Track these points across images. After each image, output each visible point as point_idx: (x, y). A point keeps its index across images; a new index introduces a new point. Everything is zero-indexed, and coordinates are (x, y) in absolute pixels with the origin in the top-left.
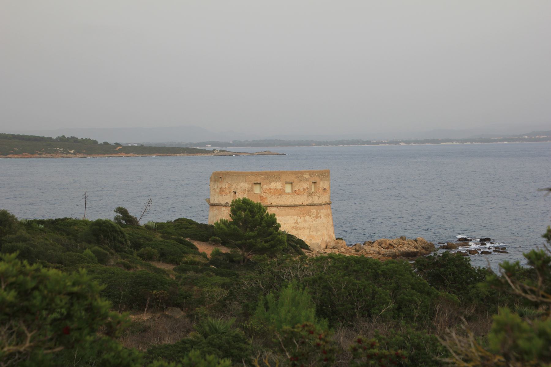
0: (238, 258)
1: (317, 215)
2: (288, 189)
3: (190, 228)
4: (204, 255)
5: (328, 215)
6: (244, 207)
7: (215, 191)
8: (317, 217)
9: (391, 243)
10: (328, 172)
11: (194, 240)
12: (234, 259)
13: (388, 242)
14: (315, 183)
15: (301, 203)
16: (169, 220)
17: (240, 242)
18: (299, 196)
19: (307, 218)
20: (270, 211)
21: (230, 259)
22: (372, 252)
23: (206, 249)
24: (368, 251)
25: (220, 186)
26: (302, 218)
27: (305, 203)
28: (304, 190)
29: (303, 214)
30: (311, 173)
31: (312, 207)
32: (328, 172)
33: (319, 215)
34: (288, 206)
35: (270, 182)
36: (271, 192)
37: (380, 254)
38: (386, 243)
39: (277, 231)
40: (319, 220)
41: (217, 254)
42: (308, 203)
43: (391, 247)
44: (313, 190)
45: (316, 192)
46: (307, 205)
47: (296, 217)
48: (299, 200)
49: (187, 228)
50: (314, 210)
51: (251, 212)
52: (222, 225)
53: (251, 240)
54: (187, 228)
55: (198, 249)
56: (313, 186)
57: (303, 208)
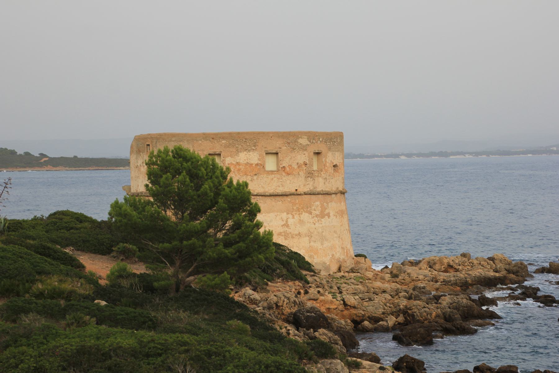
0: (163, 283)
1: (322, 212)
2: (271, 164)
3: (77, 229)
4: (92, 280)
5: (341, 213)
6: (178, 165)
7: (139, 170)
8: (322, 215)
9: (452, 263)
10: (340, 136)
11: (83, 251)
12: (156, 284)
13: (446, 261)
14: (318, 154)
15: (293, 191)
16: (39, 215)
17: (166, 245)
18: (290, 177)
19: (305, 216)
20: (236, 177)
21: (147, 285)
22: (421, 277)
23: (99, 267)
24: (414, 276)
26: (296, 217)
27: (301, 190)
28: (299, 166)
29: (298, 210)
30: (312, 136)
31: (313, 197)
32: (340, 136)
33: (327, 211)
34: (271, 196)
35: (238, 151)
36: (239, 170)
37: (437, 282)
38: (442, 263)
39: (251, 220)
40: (325, 221)
41: (122, 274)
42: (306, 190)
43: (451, 270)
44: (315, 168)
45: (320, 171)
46: (305, 194)
47: (284, 215)
48: (289, 187)
49: (72, 228)
50: (317, 203)
51: (193, 176)
52: (129, 209)
53: (194, 240)
54: (72, 228)
55: (84, 267)
56: (315, 159)
57: (298, 199)
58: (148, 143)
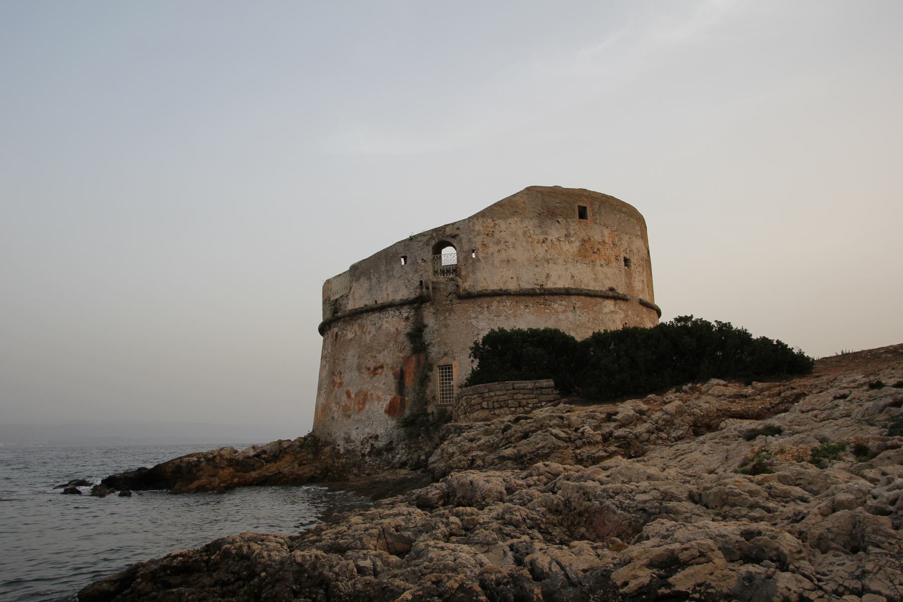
25: (583, 235)
58: (581, 204)
